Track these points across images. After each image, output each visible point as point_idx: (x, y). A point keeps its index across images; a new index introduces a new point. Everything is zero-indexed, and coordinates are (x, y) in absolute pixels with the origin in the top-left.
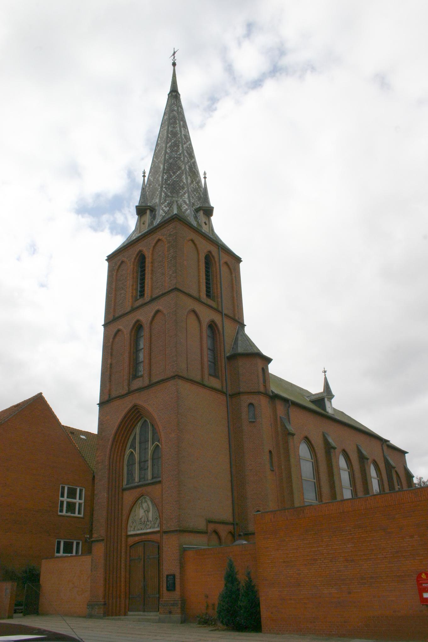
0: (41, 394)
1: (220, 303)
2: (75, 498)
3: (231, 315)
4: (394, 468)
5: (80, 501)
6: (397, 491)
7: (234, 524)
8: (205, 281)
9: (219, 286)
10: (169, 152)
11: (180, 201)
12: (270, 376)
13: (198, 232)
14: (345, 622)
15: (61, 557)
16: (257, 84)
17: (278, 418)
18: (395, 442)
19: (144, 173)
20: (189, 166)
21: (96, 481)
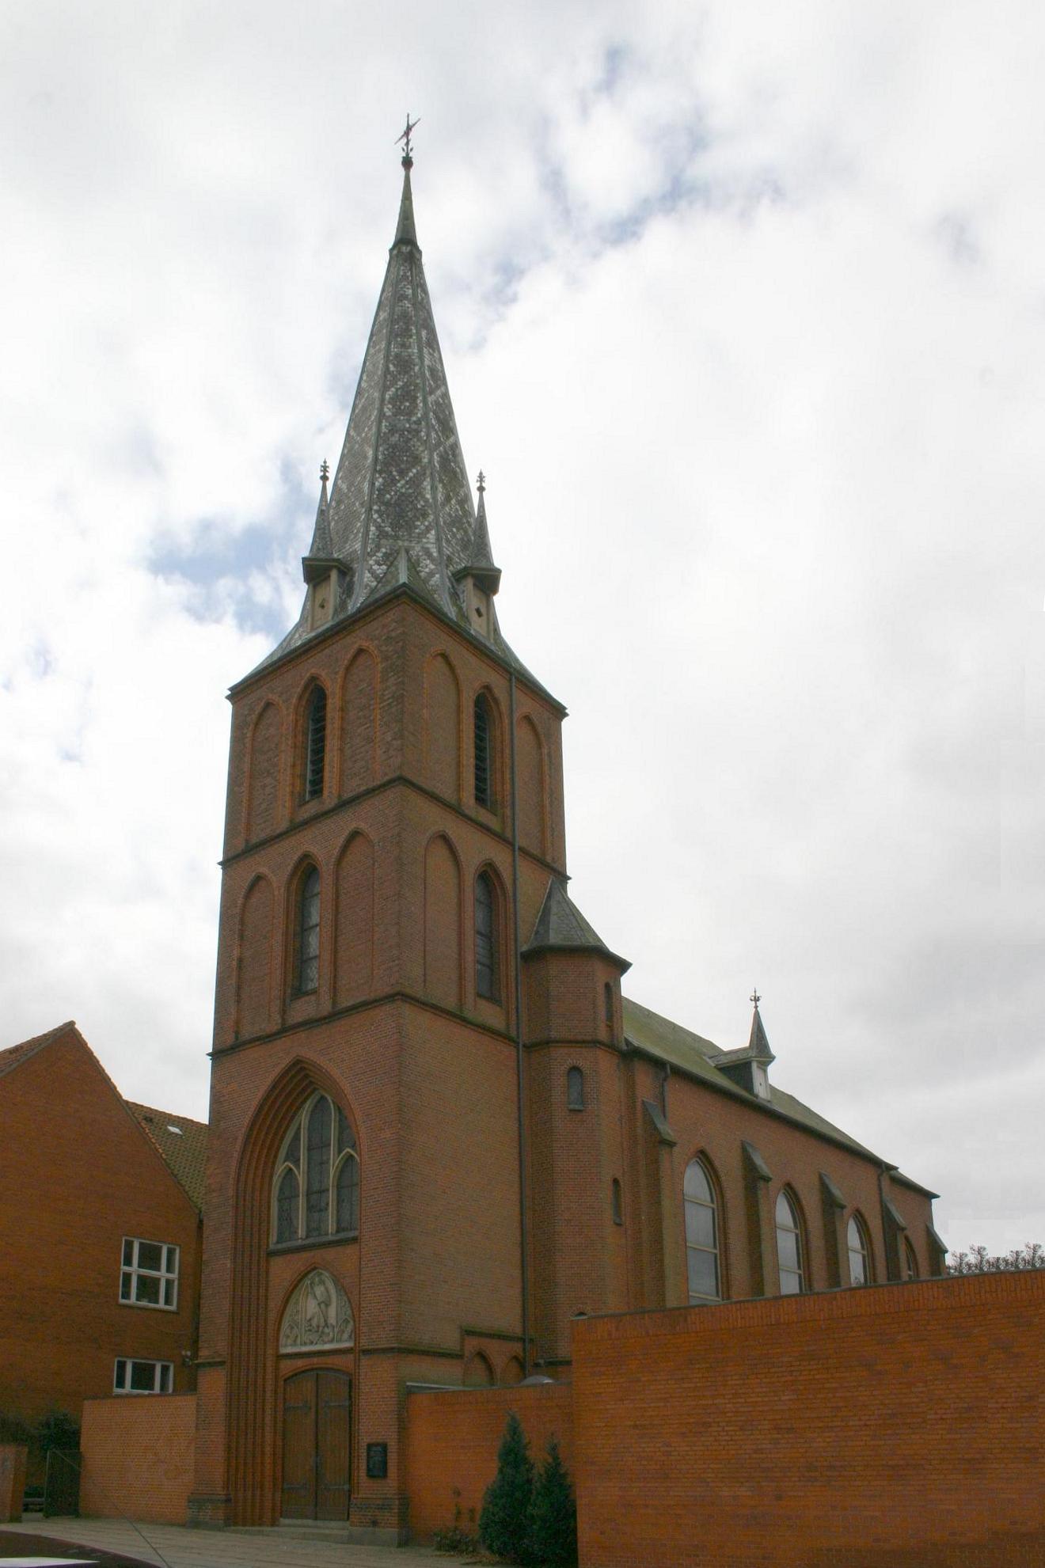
0: (72, 1023)
1: (509, 820)
2: (158, 1269)
3: (536, 852)
4: (903, 1229)
5: (170, 1276)
6: (906, 1283)
7: (524, 1341)
8: (472, 761)
9: (508, 776)
10: (389, 413)
11: (416, 550)
12: (624, 1003)
13: (459, 634)
14: (764, 1558)
15: (127, 1396)
16: (625, 230)
17: (639, 1104)
18: (911, 1169)
19: (325, 468)
20: (441, 456)
21: (206, 1232)
